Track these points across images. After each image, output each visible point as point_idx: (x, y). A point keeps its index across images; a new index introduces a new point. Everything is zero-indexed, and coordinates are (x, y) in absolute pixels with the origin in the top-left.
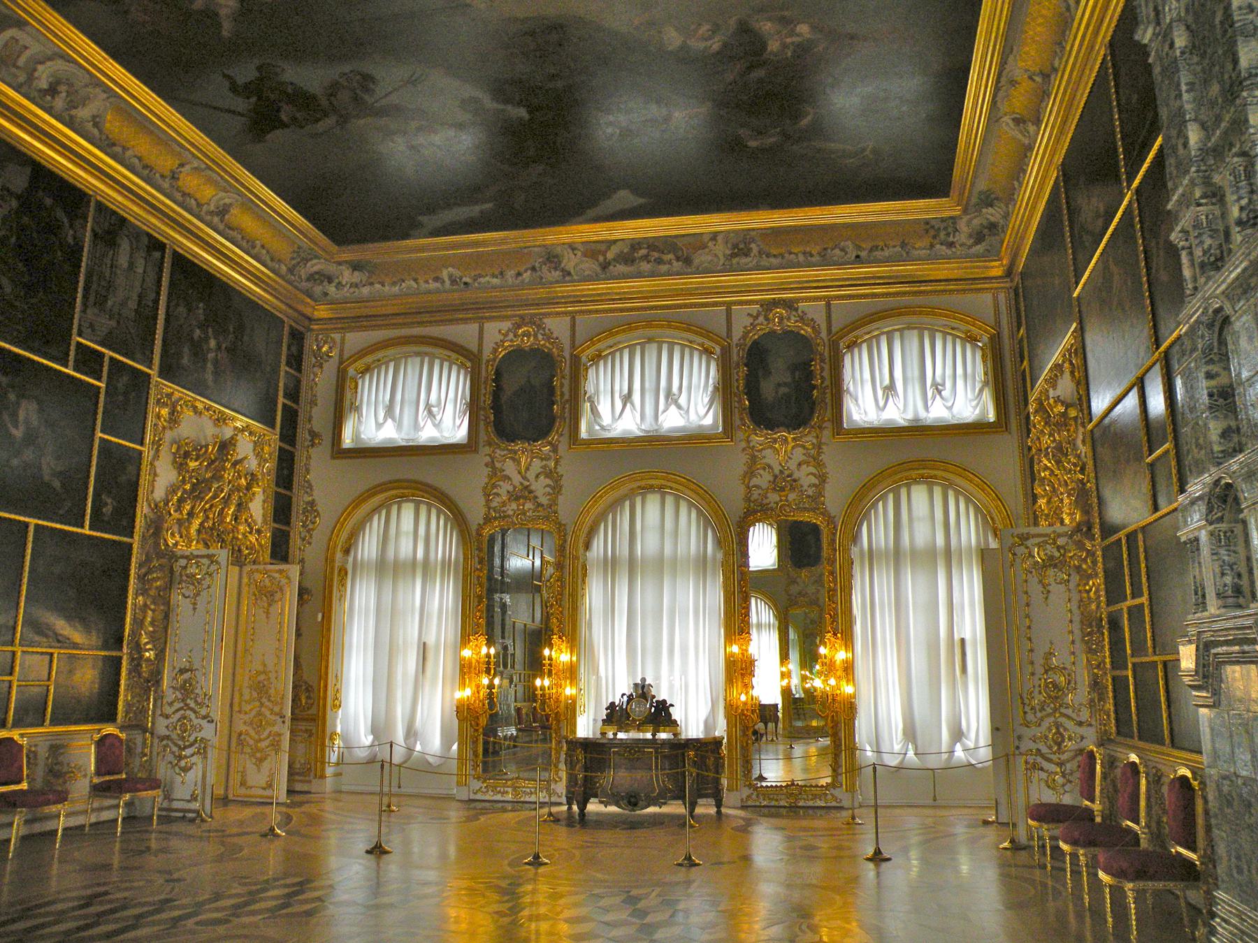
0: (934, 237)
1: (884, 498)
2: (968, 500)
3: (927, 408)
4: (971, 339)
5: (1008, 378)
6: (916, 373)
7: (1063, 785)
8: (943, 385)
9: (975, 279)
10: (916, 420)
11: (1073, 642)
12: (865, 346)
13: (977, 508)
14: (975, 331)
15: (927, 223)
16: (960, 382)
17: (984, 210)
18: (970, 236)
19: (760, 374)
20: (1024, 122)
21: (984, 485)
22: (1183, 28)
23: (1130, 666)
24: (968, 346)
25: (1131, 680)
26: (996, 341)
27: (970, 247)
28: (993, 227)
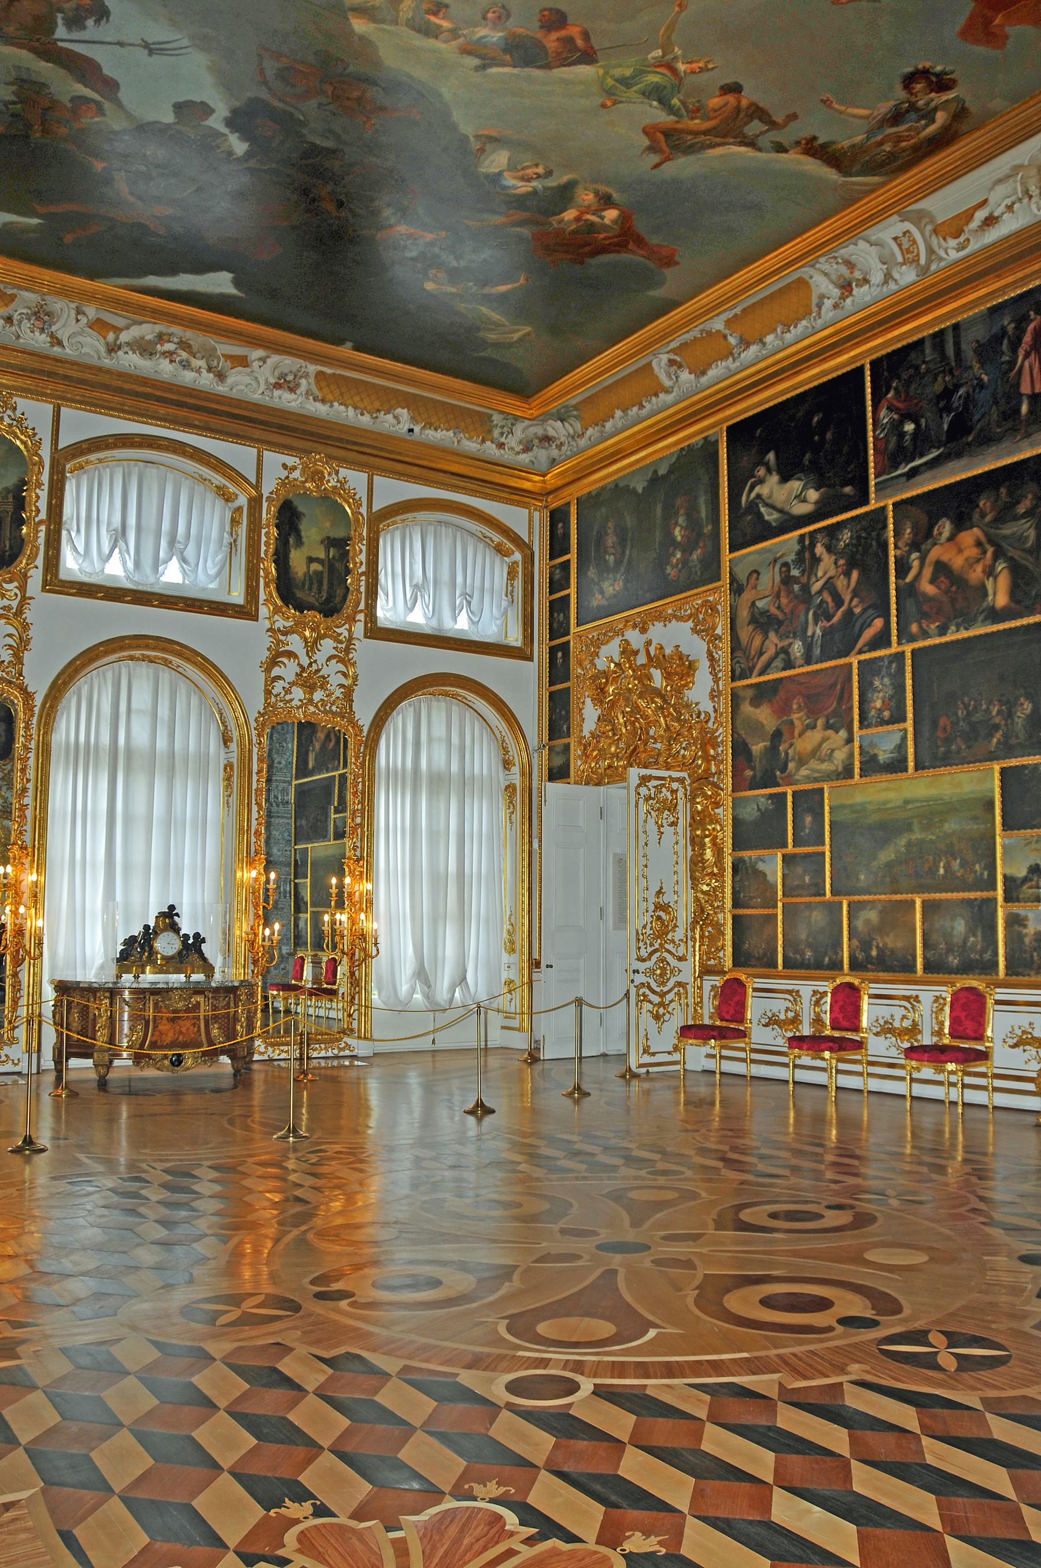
18: (520, 442)
19: (291, 541)
27: (518, 453)
28: (547, 439)
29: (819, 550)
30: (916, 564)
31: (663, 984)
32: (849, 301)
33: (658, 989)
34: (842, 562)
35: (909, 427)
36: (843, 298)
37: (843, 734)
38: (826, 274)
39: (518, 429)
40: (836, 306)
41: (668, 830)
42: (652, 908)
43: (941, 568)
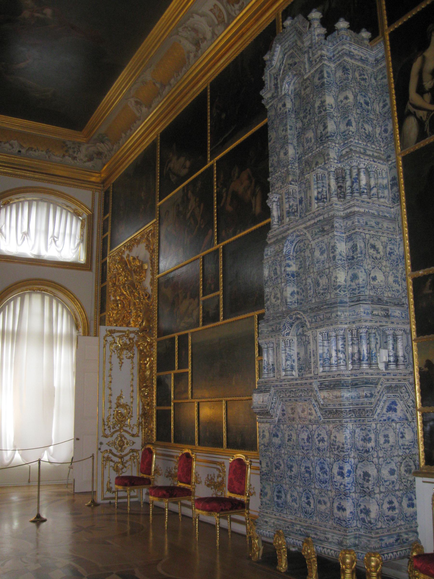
0: (67, 151)
1: (15, 299)
2: (63, 307)
3: (47, 249)
4: (76, 214)
5: (99, 240)
6: (43, 228)
7: (122, 469)
8: (58, 238)
9: (83, 180)
10: (39, 256)
11: (133, 391)
12: (14, 206)
13: (68, 312)
14: (80, 210)
15: (64, 142)
16: (67, 238)
17: (98, 144)
18: (86, 156)
20: (141, 105)
21: (74, 298)
22: (290, 100)
23: (172, 404)
24: (74, 219)
25: (172, 412)
26: (91, 218)
27: (85, 162)
28: (99, 154)
29: (190, 194)
30: (224, 195)
31: (121, 451)
32: (200, 52)
33: (118, 454)
34: (197, 199)
35: (224, 116)
36: (197, 51)
37: (196, 300)
38: (187, 39)
39: (83, 149)
40: (195, 56)
41: (127, 362)
42: (114, 406)
43: (235, 195)
